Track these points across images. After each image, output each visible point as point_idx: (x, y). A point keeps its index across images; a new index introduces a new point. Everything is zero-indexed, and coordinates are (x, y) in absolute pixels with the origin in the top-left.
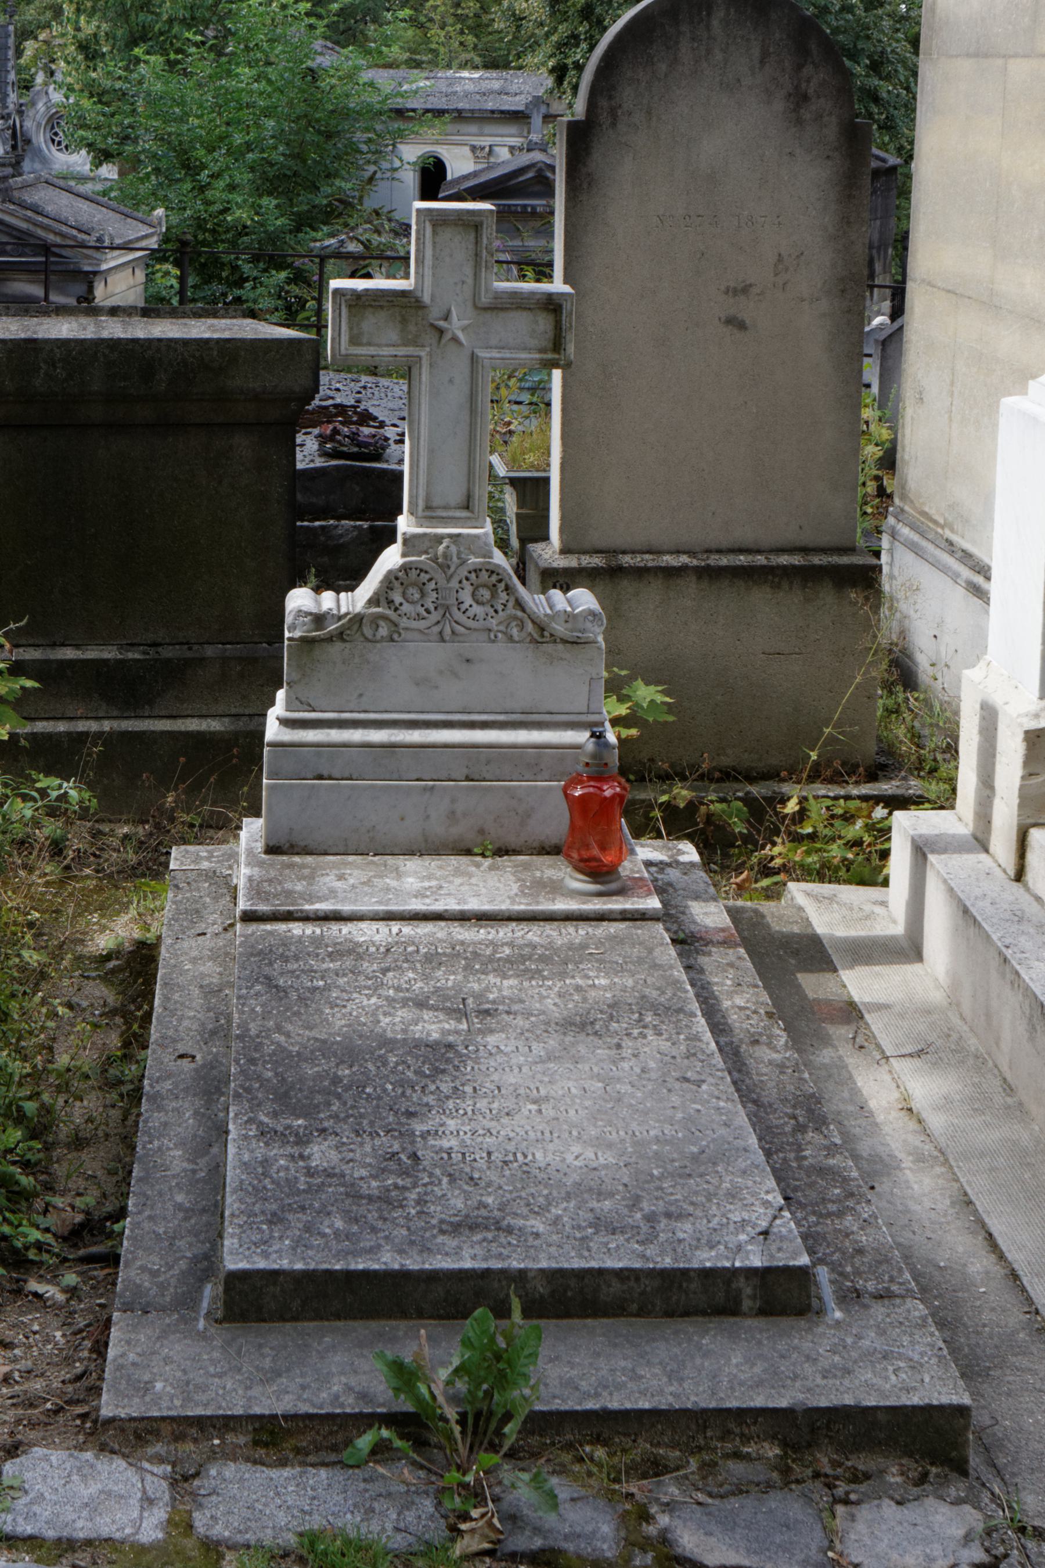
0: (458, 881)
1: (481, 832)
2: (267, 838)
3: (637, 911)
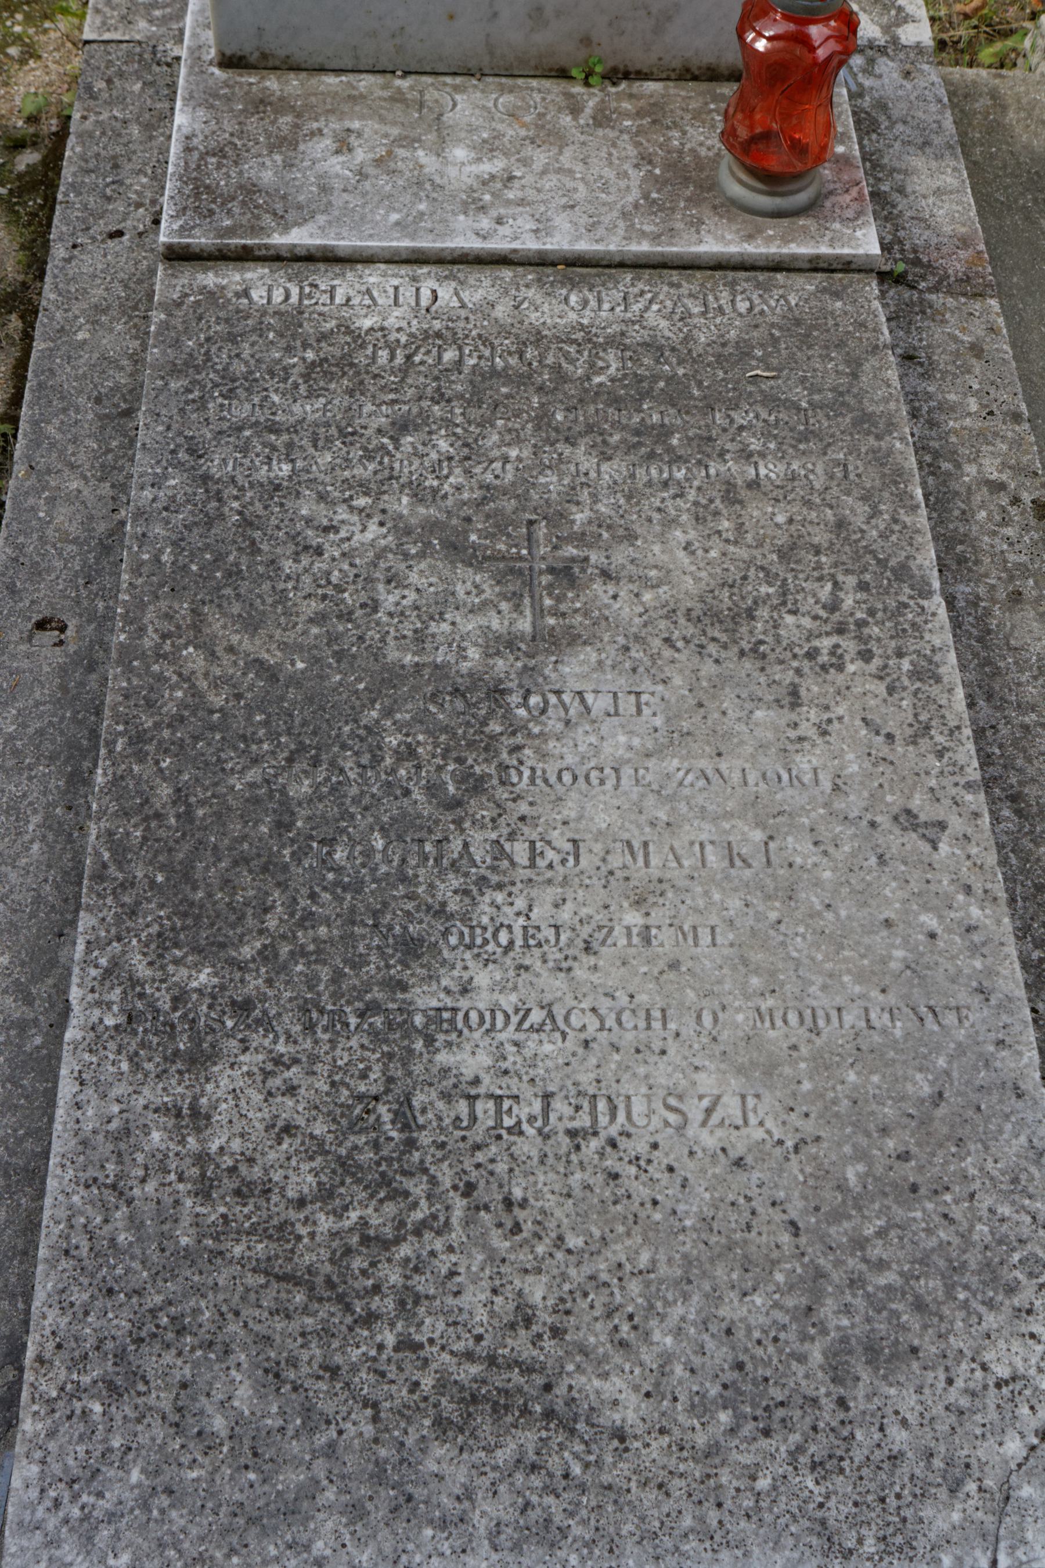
0: (540, 158)
1: (586, 41)
2: (220, 39)
3: (838, 257)
